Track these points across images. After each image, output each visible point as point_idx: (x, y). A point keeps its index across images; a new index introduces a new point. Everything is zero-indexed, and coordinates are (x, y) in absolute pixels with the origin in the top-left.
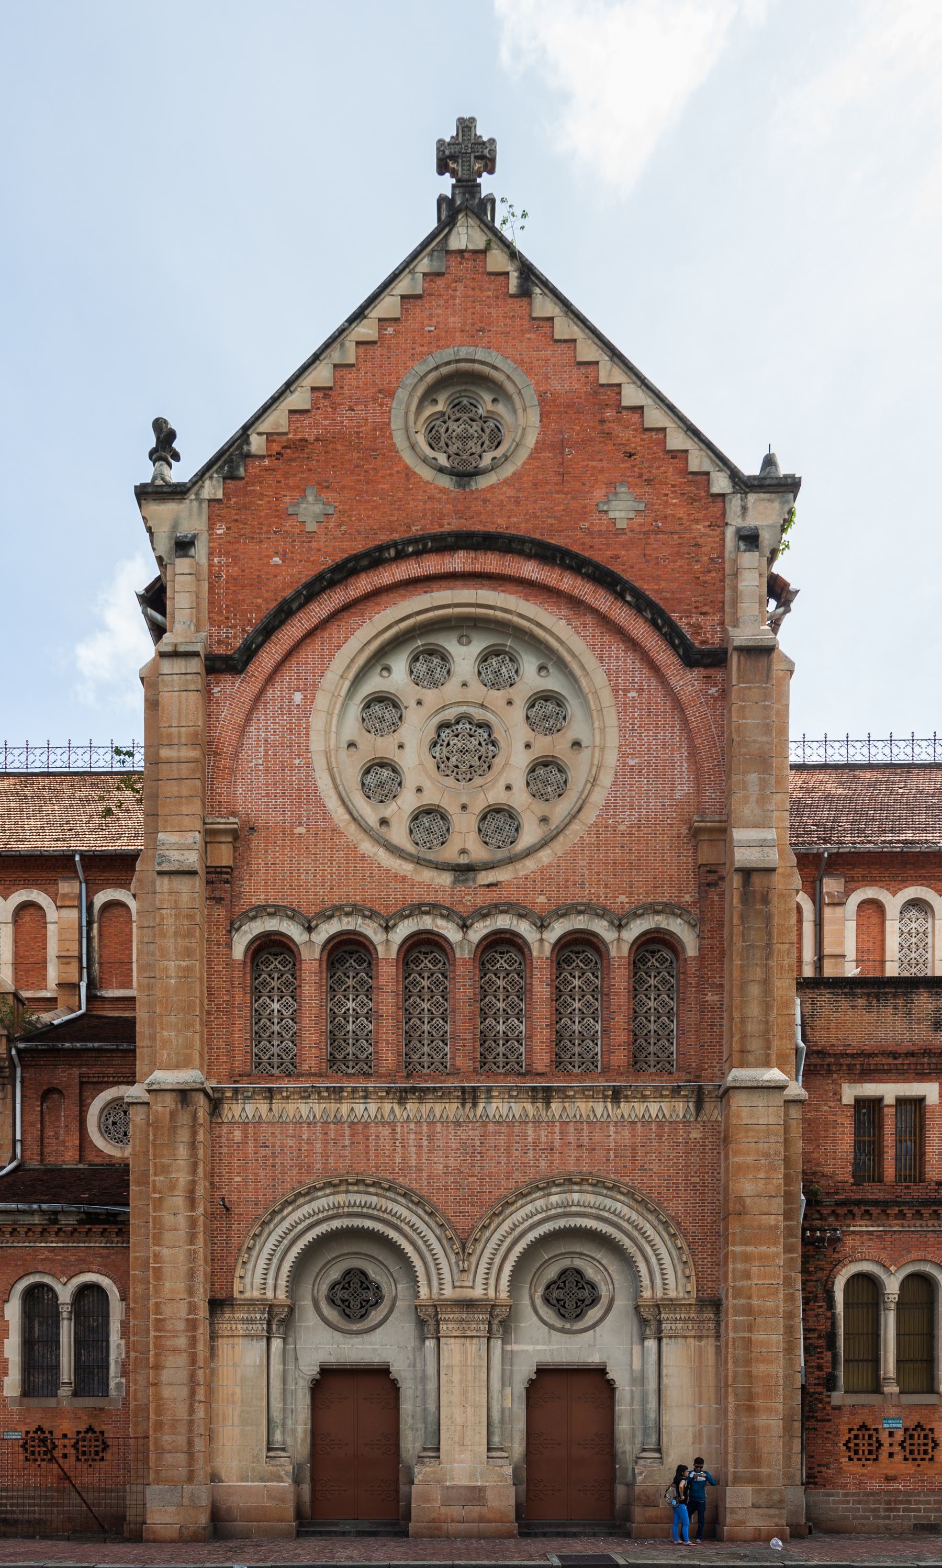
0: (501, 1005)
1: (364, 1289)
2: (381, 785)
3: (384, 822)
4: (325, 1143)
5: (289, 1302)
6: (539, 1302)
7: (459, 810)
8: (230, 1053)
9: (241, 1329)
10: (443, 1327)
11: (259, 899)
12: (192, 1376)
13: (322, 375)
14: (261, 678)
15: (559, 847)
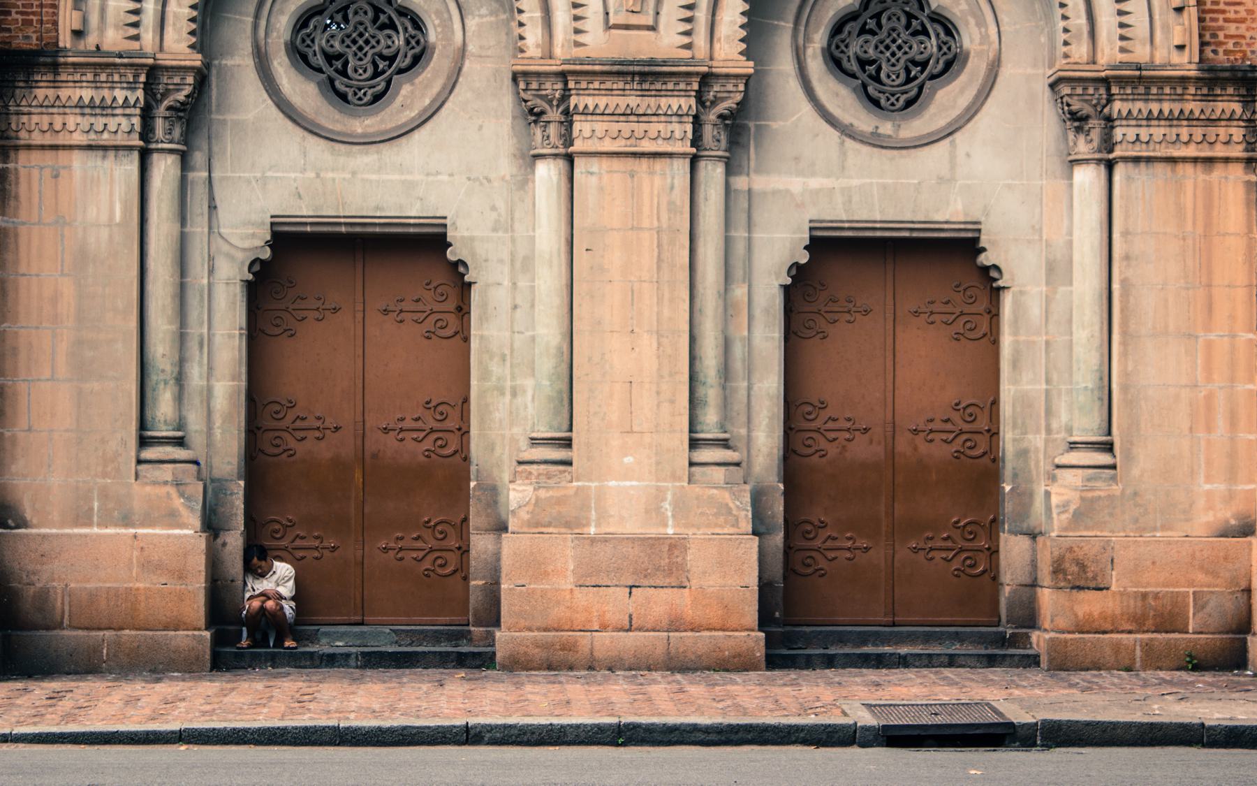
1: (382, 27)
5: (196, 60)
6: (816, 66)
9: (76, 128)
10: (581, 127)
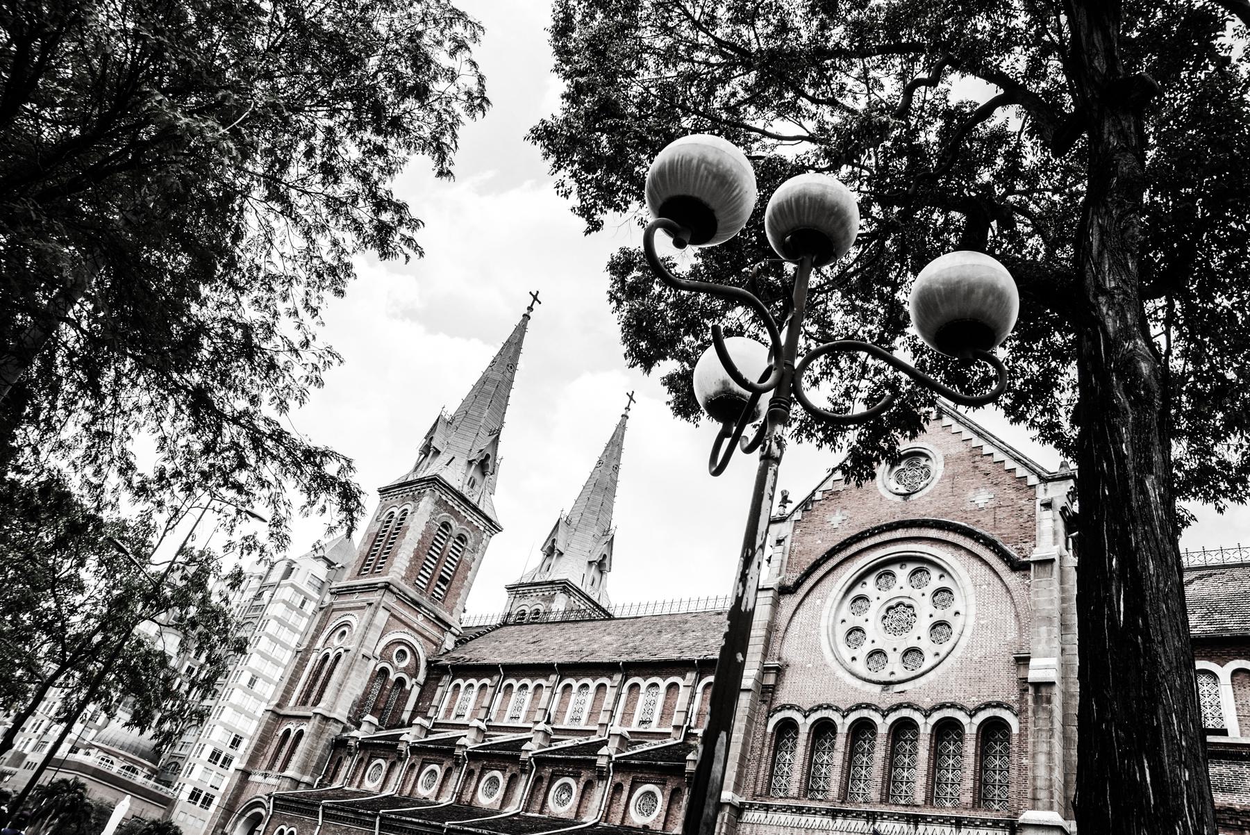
3: (854, 659)
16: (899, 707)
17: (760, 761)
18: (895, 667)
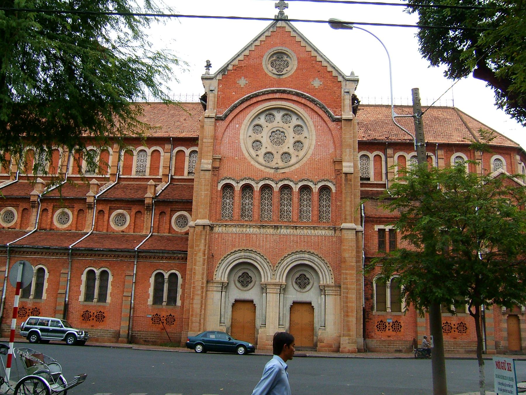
0: (286, 202)
2: (257, 146)
4: (239, 239)
5: (228, 282)
6: (294, 283)
7: (276, 153)
8: (216, 215)
9: (215, 289)
10: (268, 290)
11: (225, 175)
12: (202, 301)
13: (247, 53)
14: (229, 122)
15: (301, 164)
16: (284, 179)
17: (216, 204)
18: (277, 161)
